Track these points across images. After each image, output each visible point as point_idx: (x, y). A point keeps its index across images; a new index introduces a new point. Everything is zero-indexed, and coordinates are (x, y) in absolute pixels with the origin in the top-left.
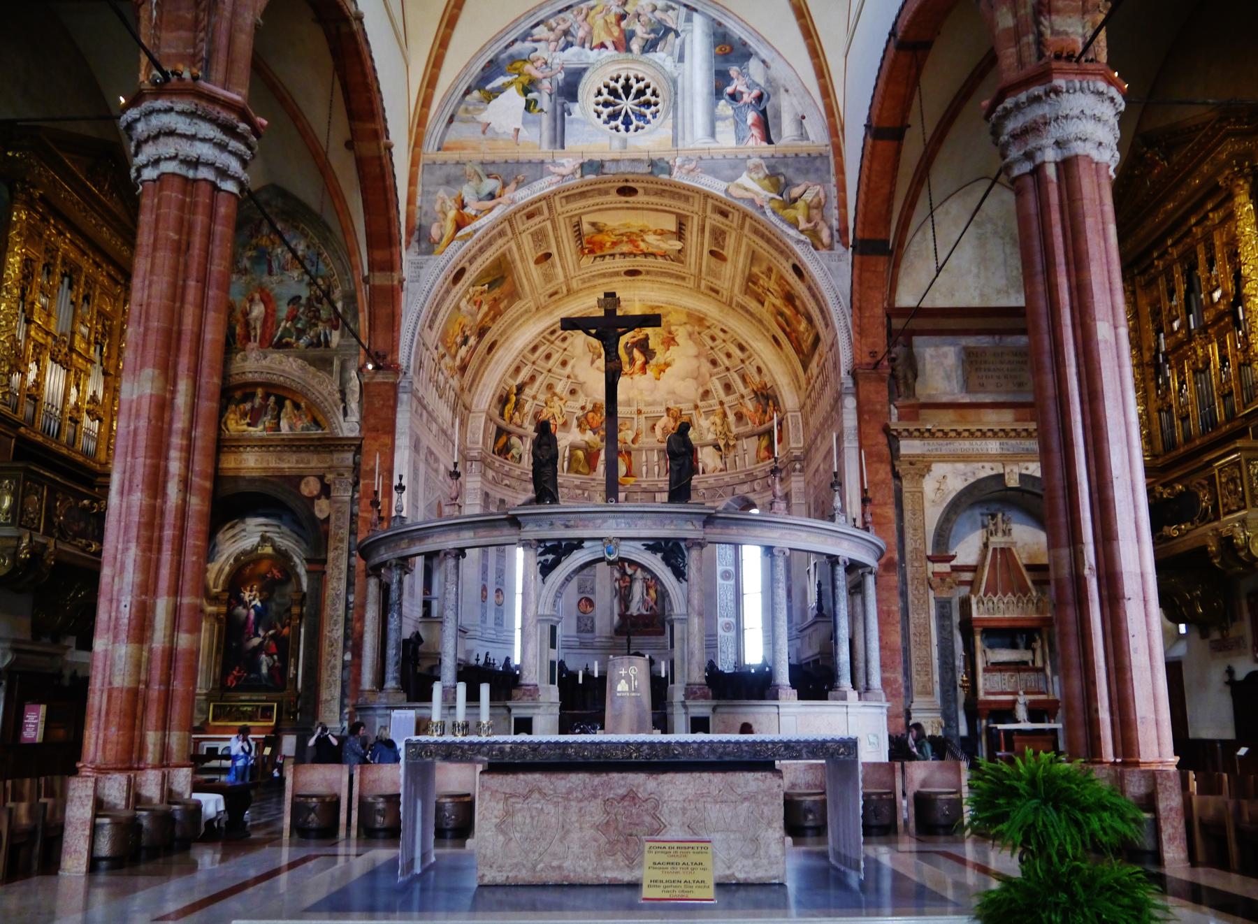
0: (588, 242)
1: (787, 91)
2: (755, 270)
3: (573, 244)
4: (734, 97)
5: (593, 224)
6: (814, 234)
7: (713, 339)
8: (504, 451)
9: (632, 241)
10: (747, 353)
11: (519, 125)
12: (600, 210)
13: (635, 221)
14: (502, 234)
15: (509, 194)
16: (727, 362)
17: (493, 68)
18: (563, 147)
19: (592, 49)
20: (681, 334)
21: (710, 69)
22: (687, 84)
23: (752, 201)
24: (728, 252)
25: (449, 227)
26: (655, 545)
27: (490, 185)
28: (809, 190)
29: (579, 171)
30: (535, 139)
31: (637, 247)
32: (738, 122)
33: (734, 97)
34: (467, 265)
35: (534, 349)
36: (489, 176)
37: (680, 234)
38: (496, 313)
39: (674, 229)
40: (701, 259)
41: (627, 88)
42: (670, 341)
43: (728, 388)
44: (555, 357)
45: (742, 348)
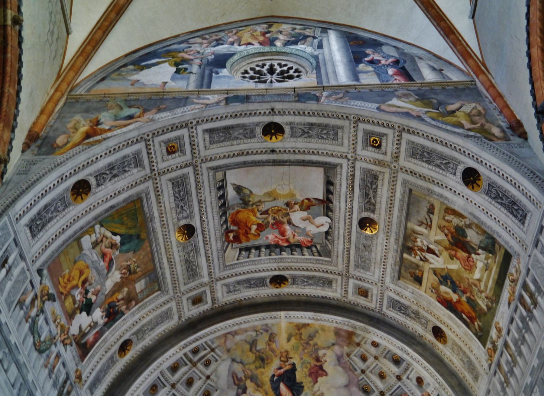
0: (234, 223)
1: (420, 58)
2: (413, 225)
3: (217, 217)
5: (239, 189)
7: (364, 359)
9: (278, 224)
10: (404, 365)
11: (167, 79)
12: (245, 164)
14: (137, 161)
15: (148, 116)
16: (381, 385)
18: (209, 85)
19: (239, 45)
21: (347, 51)
22: (327, 58)
24: (380, 216)
25: (77, 137)
29: (224, 102)
31: (283, 233)
34: (93, 181)
35: (174, 369)
36: (130, 107)
39: (321, 197)
40: (350, 233)
41: (272, 71)
44: (197, 384)
45: (397, 361)
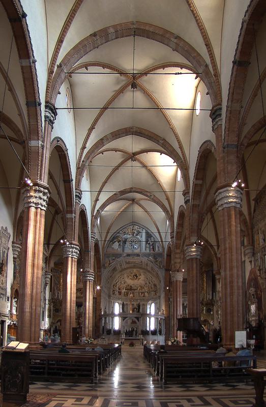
4: (149, 244)
6: (160, 266)
8: (114, 294)
13: (135, 261)
17: (114, 238)
20: (142, 274)
23: (151, 261)
26: (136, 318)
27: (114, 258)
28: (159, 259)
30: (120, 250)
32: (150, 248)
33: (149, 244)
37: (141, 262)
38: (113, 273)
42: (140, 275)
43: (149, 283)
